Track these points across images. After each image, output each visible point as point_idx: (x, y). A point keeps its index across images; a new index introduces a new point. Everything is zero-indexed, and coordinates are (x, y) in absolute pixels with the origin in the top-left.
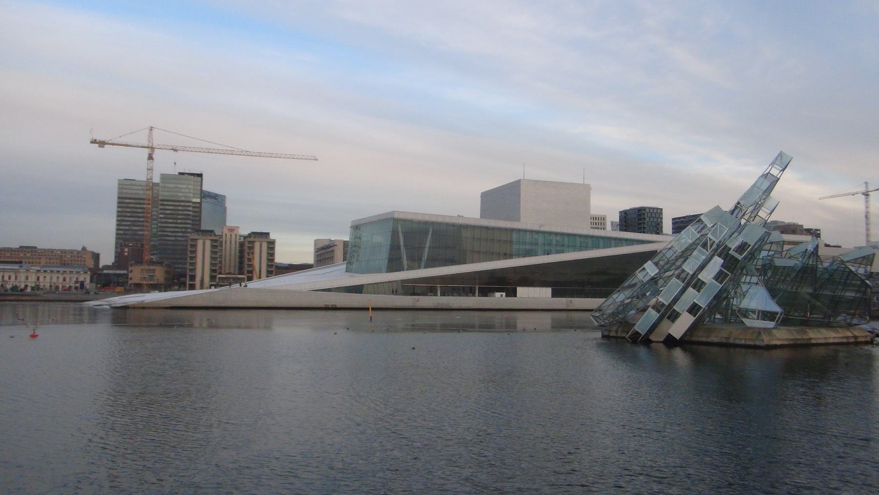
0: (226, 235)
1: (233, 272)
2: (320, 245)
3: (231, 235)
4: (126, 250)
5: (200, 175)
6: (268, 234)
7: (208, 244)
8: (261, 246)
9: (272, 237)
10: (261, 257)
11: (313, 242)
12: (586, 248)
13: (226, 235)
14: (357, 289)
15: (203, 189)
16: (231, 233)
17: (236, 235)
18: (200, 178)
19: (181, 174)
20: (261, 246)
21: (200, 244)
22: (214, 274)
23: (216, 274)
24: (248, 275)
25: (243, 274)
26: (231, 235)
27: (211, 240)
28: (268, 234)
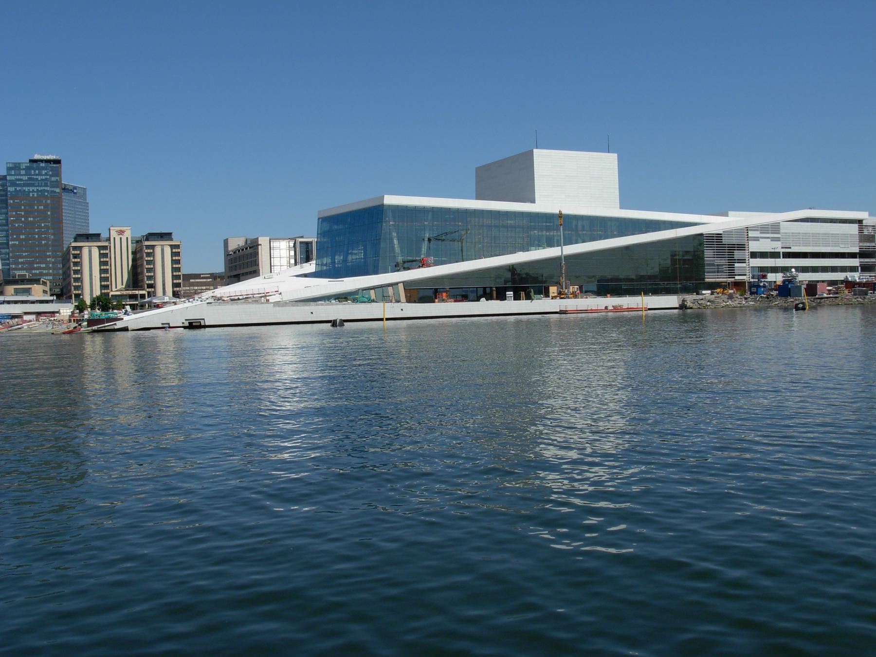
0: (114, 238)
3: (121, 238)
7: (96, 252)
11: (223, 241)
12: (622, 234)
13: (114, 238)
16: (121, 236)
17: (127, 238)
21: (85, 251)
22: (106, 291)
23: (108, 291)
24: (148, 290)
26: (121, 238)
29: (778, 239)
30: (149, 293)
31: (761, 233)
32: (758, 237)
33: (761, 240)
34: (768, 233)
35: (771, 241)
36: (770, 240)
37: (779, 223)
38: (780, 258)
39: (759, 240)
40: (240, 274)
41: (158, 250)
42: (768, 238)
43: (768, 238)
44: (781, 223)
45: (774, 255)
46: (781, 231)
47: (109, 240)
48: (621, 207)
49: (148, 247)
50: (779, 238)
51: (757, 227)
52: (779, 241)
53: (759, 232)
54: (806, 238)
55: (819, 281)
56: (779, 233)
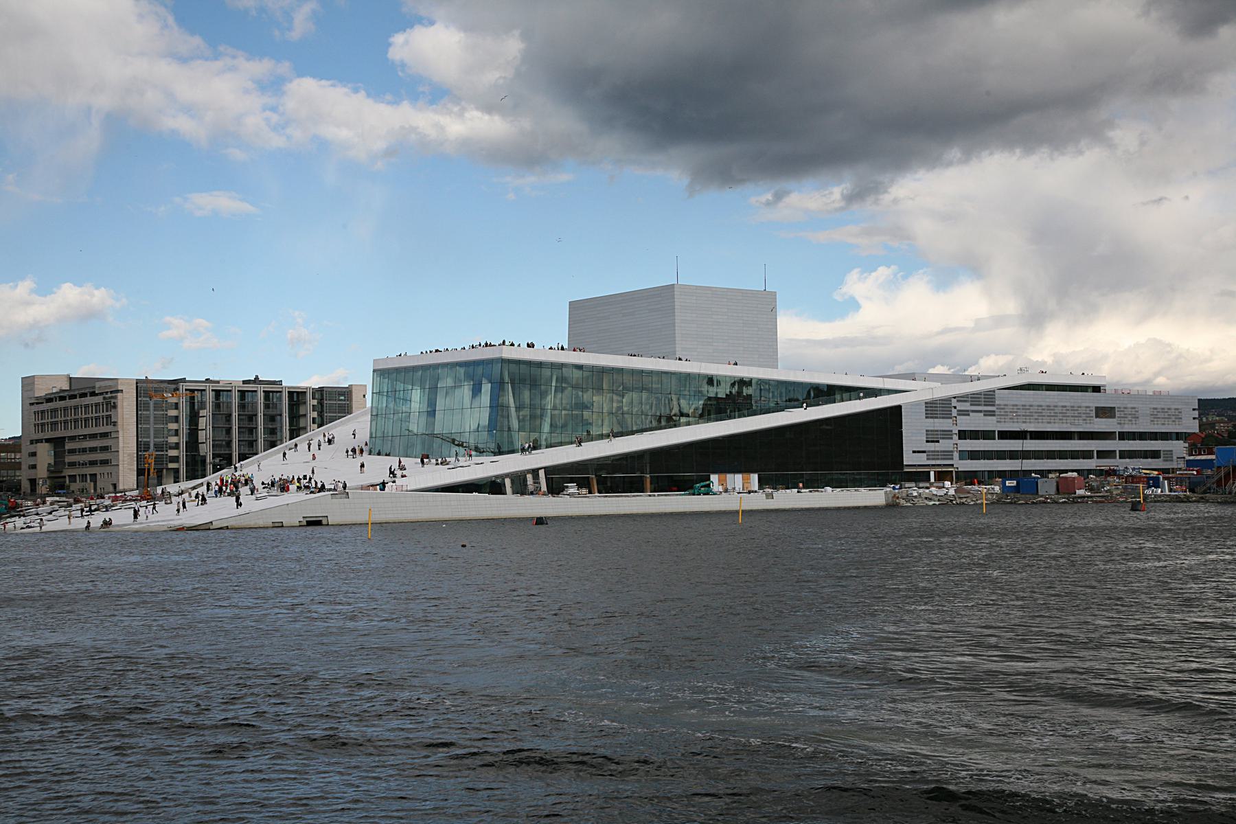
2: (41, 391)
29: (992, 414)
31: (971, 405)
32: (968, 411)
33: (971, 414)
34: (979, 405)
35: (985, 415)
36: (982, 414)
37: (994, 391)
38: (994, 439)
39: (969, 415)
40: (65, 437)
42: (980, 411)
43: (980, 411)
44: (997, 392)
45: (987, 435)
46: (997, 402)
50: (994, 411)
51: (966, 396)
52: (994, 415)
53: (968, 404)
56: (994, 405)
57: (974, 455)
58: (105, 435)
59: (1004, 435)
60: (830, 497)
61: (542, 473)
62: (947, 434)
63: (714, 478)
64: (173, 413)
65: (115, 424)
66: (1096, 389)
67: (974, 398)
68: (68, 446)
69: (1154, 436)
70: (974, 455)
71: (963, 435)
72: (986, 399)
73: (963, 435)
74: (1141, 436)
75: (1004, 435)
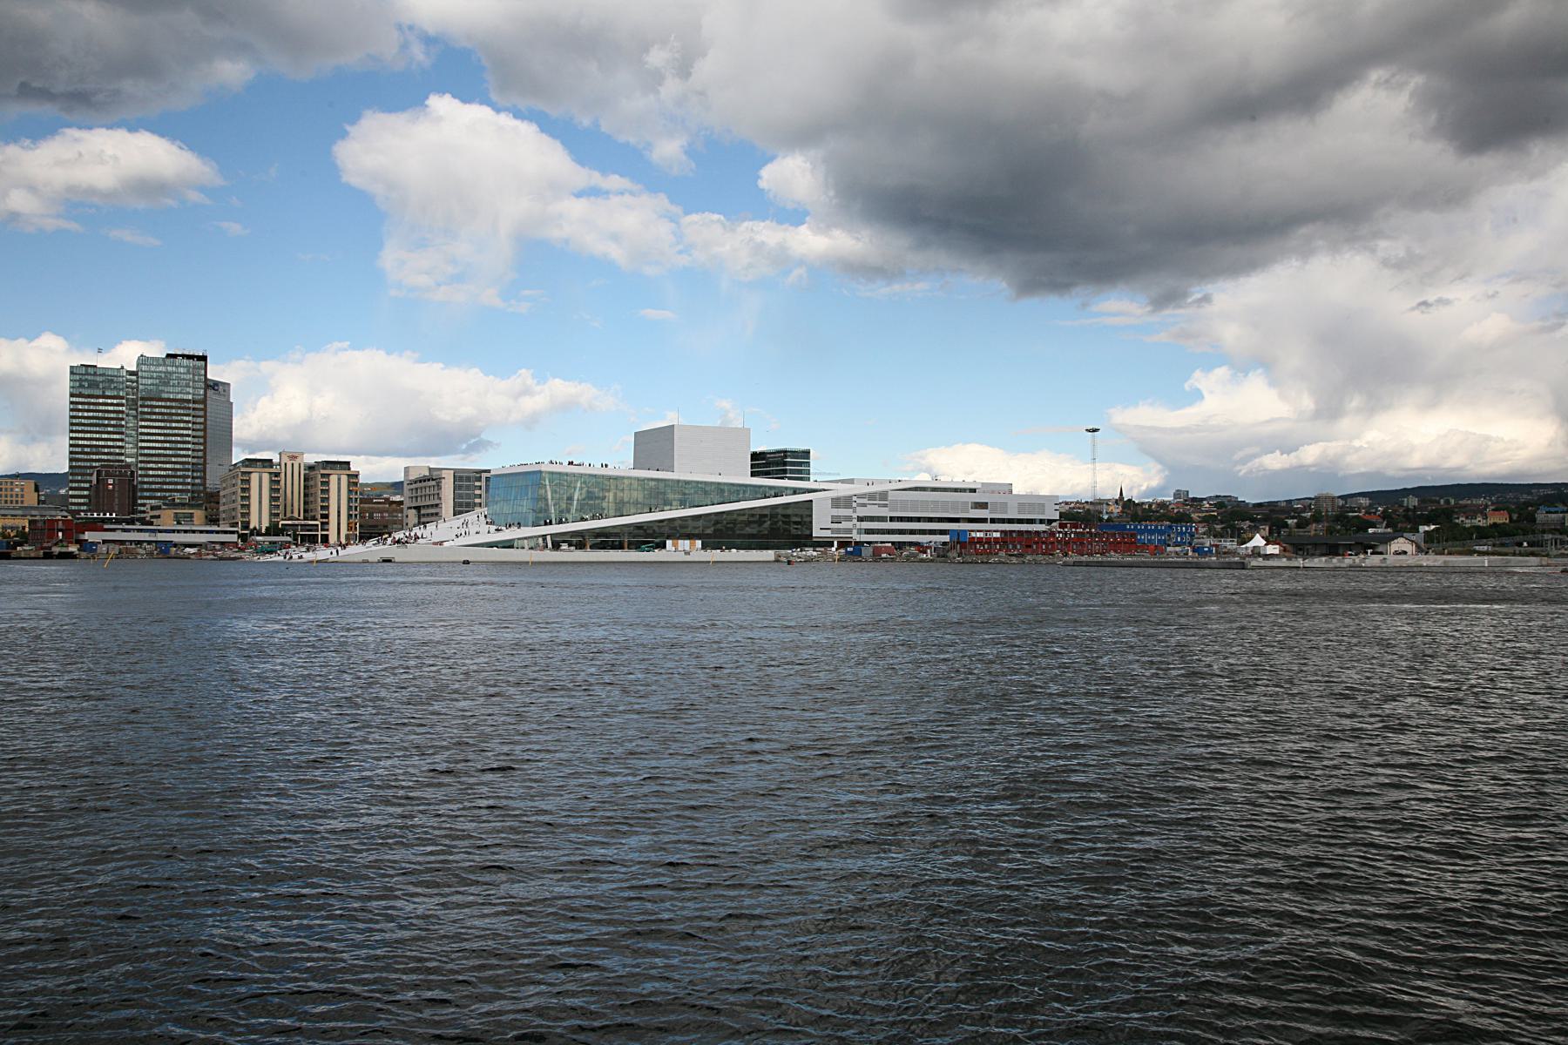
1: (296, 515)
4: (111, 481)
5: (204, 358)
6: (348, 463)
7: (266, 477)
8: (339, 479)
9: (353, 468)
10: (339, 496)
14: (508, 545)
15: (209, 377)
18: (203, 363)
19: (169, 356)
20: (339, 479)
25: (314, 519)
27: (270, 473)
28: (348, 463)
29: (885, 506)
30: (322, 523)
41: (334, 479)
47: (280, 464)
48: (753, 474)
49: (323, 475)
54: (915, 505)
55: (905, 542)
57: (868, 532)
58: (437, 505)
59: (892, 519)
60: (734, 555)
61: (549, 538)
62: (849, 519)
63: (669, 543)
64: (477, 492)
65: (440, 499)
66: (973, 491)
67: (872, 496)
68: (423, 512)
69: (1020, 521)
70: (868, 532)
71: (860, 519)
72: (883, 495)
73: (860, 519)
74: (1010, 521)
75: (892, 519)
